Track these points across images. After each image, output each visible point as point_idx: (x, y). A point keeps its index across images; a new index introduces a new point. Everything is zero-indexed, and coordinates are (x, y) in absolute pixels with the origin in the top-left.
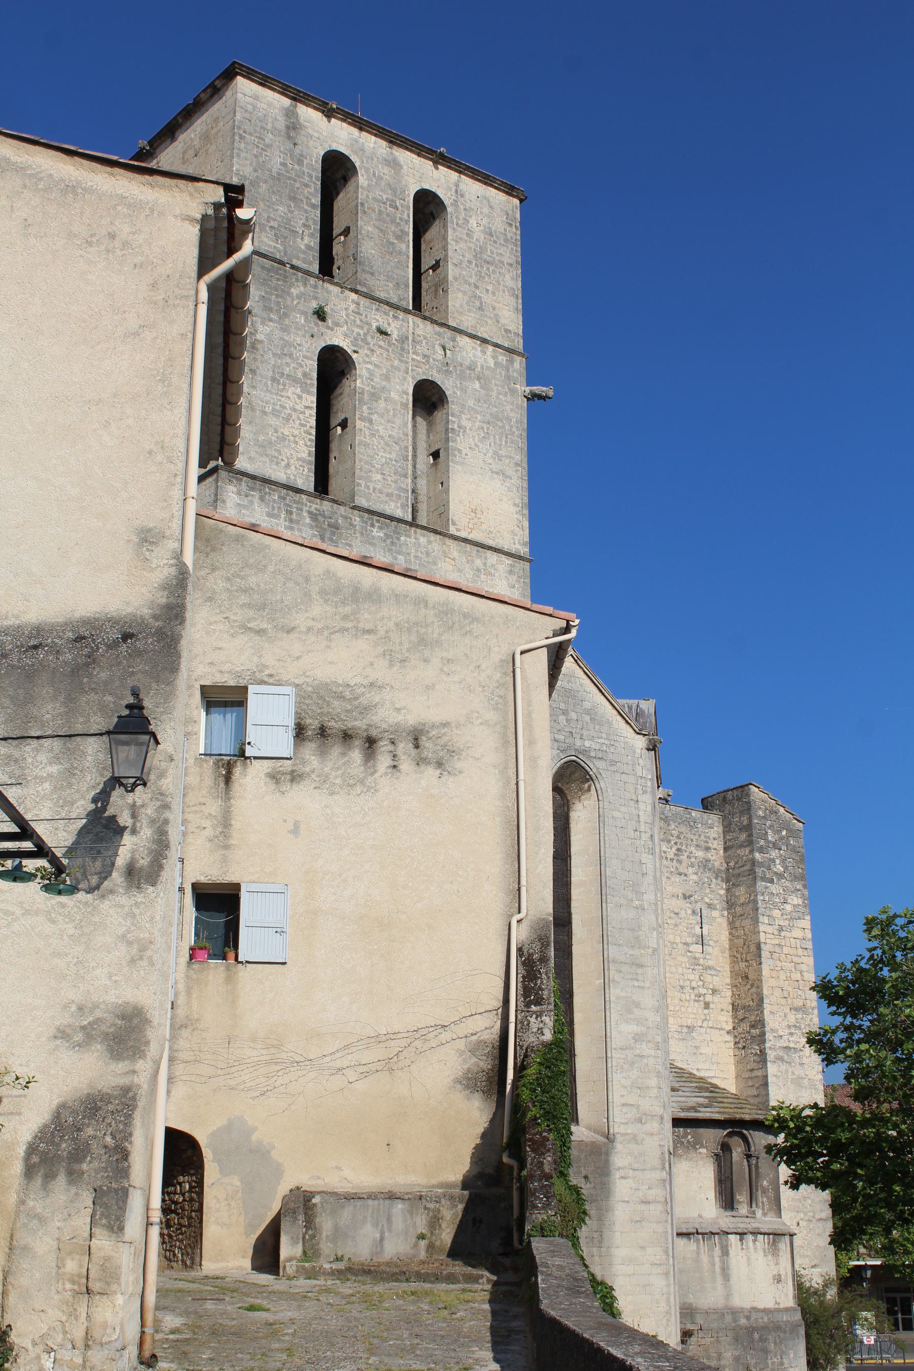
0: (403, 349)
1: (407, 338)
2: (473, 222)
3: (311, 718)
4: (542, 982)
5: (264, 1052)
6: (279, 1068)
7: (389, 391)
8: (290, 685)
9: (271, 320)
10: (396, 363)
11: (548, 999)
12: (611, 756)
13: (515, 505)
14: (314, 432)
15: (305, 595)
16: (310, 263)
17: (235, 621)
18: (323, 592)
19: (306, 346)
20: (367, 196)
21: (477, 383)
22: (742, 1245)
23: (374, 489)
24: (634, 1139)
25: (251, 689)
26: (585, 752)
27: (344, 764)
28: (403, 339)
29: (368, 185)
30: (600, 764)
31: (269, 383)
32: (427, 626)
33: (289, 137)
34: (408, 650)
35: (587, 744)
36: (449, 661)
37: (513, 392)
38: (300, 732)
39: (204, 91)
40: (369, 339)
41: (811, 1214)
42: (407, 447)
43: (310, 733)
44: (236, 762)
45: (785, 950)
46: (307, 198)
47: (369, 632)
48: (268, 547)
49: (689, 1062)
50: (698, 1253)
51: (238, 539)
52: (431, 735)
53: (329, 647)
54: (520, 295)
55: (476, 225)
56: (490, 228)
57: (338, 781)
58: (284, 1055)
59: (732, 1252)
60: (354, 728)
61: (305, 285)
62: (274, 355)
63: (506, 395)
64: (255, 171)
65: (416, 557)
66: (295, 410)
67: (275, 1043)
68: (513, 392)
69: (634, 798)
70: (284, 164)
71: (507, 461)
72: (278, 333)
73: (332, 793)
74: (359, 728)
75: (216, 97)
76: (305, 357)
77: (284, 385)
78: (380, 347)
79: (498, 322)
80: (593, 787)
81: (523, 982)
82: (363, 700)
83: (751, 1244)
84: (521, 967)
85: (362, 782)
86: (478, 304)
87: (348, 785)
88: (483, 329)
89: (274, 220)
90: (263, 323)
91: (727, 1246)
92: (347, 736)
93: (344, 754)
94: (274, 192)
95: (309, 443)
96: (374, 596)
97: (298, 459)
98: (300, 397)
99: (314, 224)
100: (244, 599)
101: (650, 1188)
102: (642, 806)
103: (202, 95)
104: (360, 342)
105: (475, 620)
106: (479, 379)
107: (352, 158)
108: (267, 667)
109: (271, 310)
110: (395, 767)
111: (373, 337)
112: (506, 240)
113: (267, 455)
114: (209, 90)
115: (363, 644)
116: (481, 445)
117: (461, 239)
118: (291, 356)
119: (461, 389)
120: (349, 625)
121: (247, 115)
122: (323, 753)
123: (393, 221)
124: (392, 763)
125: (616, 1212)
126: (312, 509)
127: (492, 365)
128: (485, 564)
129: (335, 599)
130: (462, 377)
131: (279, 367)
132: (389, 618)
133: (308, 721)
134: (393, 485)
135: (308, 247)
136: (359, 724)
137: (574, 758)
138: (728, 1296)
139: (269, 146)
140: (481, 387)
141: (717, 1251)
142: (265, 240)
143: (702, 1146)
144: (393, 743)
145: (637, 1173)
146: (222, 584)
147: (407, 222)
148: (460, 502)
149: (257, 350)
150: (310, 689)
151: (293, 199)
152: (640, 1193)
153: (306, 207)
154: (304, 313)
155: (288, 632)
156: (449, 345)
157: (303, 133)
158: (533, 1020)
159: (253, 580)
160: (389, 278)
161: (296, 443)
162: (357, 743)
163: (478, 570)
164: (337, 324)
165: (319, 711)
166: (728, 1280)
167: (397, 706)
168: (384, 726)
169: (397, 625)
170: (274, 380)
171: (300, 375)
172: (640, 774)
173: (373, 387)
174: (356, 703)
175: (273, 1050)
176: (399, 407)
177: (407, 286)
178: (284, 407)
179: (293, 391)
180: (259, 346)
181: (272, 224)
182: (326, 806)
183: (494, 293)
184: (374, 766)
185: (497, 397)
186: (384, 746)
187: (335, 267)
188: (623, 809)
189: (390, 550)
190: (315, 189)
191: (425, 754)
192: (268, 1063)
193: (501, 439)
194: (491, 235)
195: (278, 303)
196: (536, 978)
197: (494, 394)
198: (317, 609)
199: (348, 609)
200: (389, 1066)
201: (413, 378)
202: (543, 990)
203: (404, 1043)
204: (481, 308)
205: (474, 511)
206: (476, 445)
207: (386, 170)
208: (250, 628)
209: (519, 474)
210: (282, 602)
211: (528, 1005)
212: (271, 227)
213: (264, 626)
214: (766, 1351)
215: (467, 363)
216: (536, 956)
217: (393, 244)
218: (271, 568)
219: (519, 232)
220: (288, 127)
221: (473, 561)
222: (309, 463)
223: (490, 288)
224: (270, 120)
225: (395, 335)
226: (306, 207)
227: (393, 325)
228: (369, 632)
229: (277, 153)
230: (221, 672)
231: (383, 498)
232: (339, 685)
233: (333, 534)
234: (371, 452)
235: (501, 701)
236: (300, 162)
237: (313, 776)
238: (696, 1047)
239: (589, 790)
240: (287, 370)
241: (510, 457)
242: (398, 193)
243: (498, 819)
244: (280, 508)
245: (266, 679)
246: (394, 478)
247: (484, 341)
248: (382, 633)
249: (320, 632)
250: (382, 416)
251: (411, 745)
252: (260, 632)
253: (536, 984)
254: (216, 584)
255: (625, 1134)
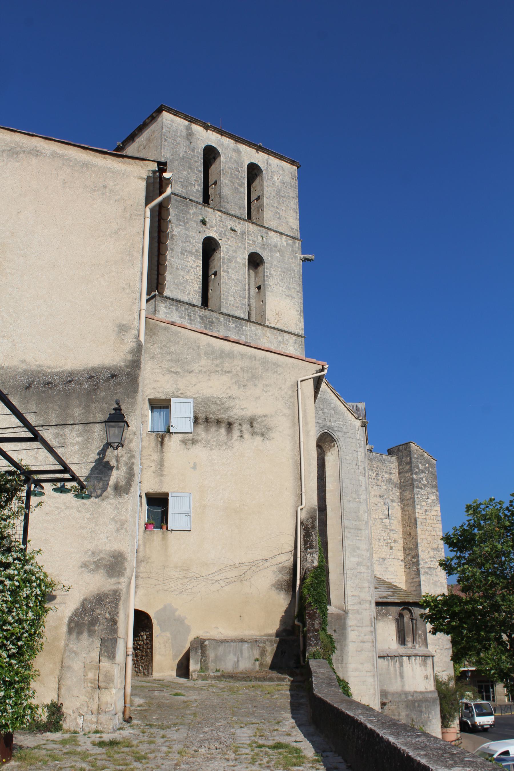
0: (243, 238)
1: (245, 233)
2: (275, 178)
3: (201, 413)
4: (313, 538)
5: (181, 573)
6: (188, 580)
7: (237, 258)
8: (191, 398)
9: (180, 225)
10: (240, 244)
11: (316, 546)
12: (344, 430)
13: (297, 311)
14: (201, 278)
15: (198, 355)
16: (198, 198)
17: (164, 368)
18: (206, 354)
19: (197, 237)
20: (225, 166)
21: (278, 253)
23: (230, 304)
24: (358, 612)
25: (173, 400)
26: (332, 428)
27: (217, 435)
28: (243, 233)
29: (226, 161)
30: (339, 434)
31: (180, 255)
32: (256, 369)
33: (188, 139)
34: (247, 380)
35: (333, 424)
36: (266, 385)
37: (295, 257)
38: (196, 420)
39: (148, 118)
40: (227, 233)
41: (442, 646)
42: (245, 284)
43: (201, 421)
44: (166, 435)
45: (428, 521)
46: (197, 168)
47: (228, 372)
48: (180, 332)
50: (388, 666)
51: (165, 329)
52: (258, 421)
53: (209, 380)
54: (298, 212)
55: (276, 179)
56: (283, 181)
57: (215, 443)
58: (190, 574)
59: (405, 665)
60: (222, 418)
61: (196, 208)
62: (182, 241)
63: (292, 259)
64: (172, 155)
65: (250, 336)
66: (192, 267)
67: (186, 568)
68: (295, 257)
69: (356, 449)
70: (185, 152)
71: (293, 290)
72: (183, 231)
73: (212, 449)
74: (224, 418)
75: (153, 121)
76: (196, 242)
77: (187, 256)
78: (232, 237)
79: (288, 224)
80: (336, 445)
81: (303, 538)
82: (226, 405)
83: (413, 661)
84: (302, 531)
85: (226, 443)
86: (278, 216)
87: (219, 445)
88: (280, 228)
89: (181, 178)
90: (176, 227)
92: (218, 422)
93: (217, 431)
94: (181, 165)
95: (199, 283)
96: (230, 355)
97: (194, 291)
98: (194, 261)
99: (200, 180)
100: (168, 357)
101: (365, 635)
102: (359, 453)
103: (147, 121)
104: (222, 235)
105: (279, 366)
106: (279, 251)
107: (218, 148)
108: (180, 389)
109: (180, 220)
110: (241, 436)
111: (228, 233)
112: (291, 186)
113: (179, 289)
114: (150, 118)
115: (225, 378)
116: (280, 283)
117: (270, 186)
118: (190, 242)
119: (271, 256)
120: (219, 369)
121: (168, 129)
122: (207, 430)
123: (238, 178)
124: (240, 435)
125: (349, 647)
126: (201, 314)
127: (285, 245)
128: (283, 339)
129: (212, 357)
130: (271, 251)
131: (184, 247)
132: (238, 366)
133: (200, 415)
134: (239, 302)
135: (197, 190)
136: (224, 416)
137: (326, 431)
138: (403, 686)
139: (179, 144)
140: (280, 255)
141: (398, 665)
142: (177, 187)
143: (390, 615)
144: (240, 425)
145: (359, 628)
146: (158, 351)
147: (244, 178)
148: (271, 310)
149: (174, 239)
150: (200, 400)
151: (190, 168)
152: (360, 638)
153: (196, 172)
154: (196, 222)
155: (190, 373)
156: (265, 236)
157: (194, 137)
158: (308, 556)
159: (173, 348)
160: (236, 205)
161: (193, 283)
162: (223, 425)
163: (280, 342)
164: (211, 227)
165: (205, 410)
166: (403, 678)
167: (242, 407)
168: (236, 417)
169: (241, 368)
170: (182, 253)
171: (194, 251)
172: (358, 438)
173: (229, 256)
174: (222, 406)
175: (185, 572)
176: (241, 265)
177: (244, 208)
178: (187, 266)
179: (191, 258)
180: (175, 237)
181: (180, 180)
182: (209, 455)
183: (286, 211)
184: (231, 436)
185: (288, 260)
186: (236, 427)
187: (210, 200)
188: (350, 455)
189: (238, 333)
190: (201, 163)
191: (256, 430)
192: (183, 578)
193: (290, 280)
194: (284, 184)
195: (183, 217)
196: (310, 536)
197: (286, 259)
198: (203, 362)
199: (218, 362)
200: (240, 579)
201: (248, 251)
202: (313, 542)
203: (247, 568)
204: (279, 218)
205: (278, 314)
206: (278, 283)
207: (234, 154)
208: (172, 371)
209: (299, 296)
210: (187, 358)
211: (306, 549)
212: (180, 181)
213: (178, 370)
214: (421, 712)
215: (273, 244)
216: (310, 526)
217: (237, 188)
218: (181, 343)
219: (297, 182)
220: (187, 135)
221: (277, 338)
222: (199, 292)
223: (284, 208)
224: (179, 131)
225: (239, 232)
226: (196, 172)
227: (238, 227)
228: (228, 372)
229: (183, 147)
230: (158, 392)
231: (234, 308)
232: (214, 398)
233: (211, 326)
234: (228, 287)
235: (291, 404)
236: (193, 151)
237: (203, 441)
238: (387, 568)
239: (334, 446)
240: (188, 249)
241: (294, 288)
242: (240, 164)
243: (291, 460)
244: (185, 314)
245: (180, 395)
246: (239, 299)
247: (281, 234)
248: (234, 372)
249: (205, 372)
250: (233, 270)
251: (249, 426)
252: (177, 373)
253: (310, 539)
254: (155, 350)
255: (353, 610)
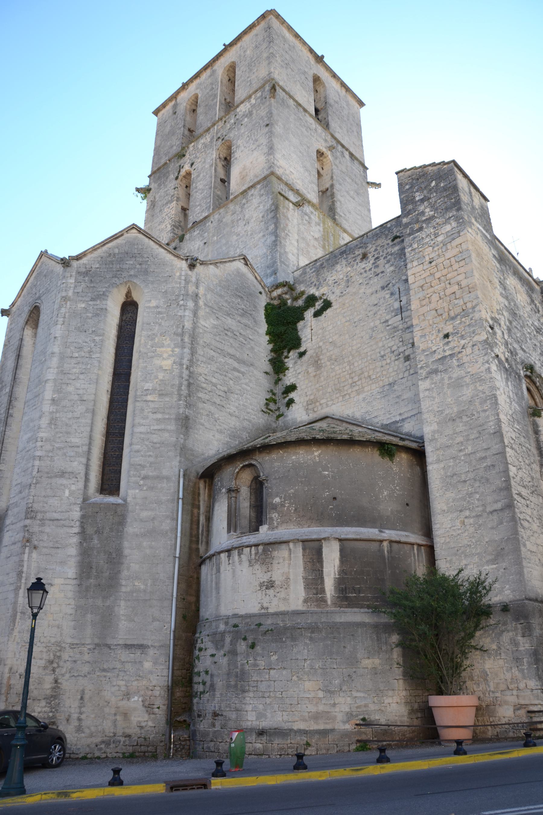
1: (214, 136)
22: (229, 561)
41: (480, 509)
45: (438, 275)
49: (392, 412)
83: (236, 558)
86: (249, 84)
91: (219, 564)
147: (218, 89)
166: (219, 593)
